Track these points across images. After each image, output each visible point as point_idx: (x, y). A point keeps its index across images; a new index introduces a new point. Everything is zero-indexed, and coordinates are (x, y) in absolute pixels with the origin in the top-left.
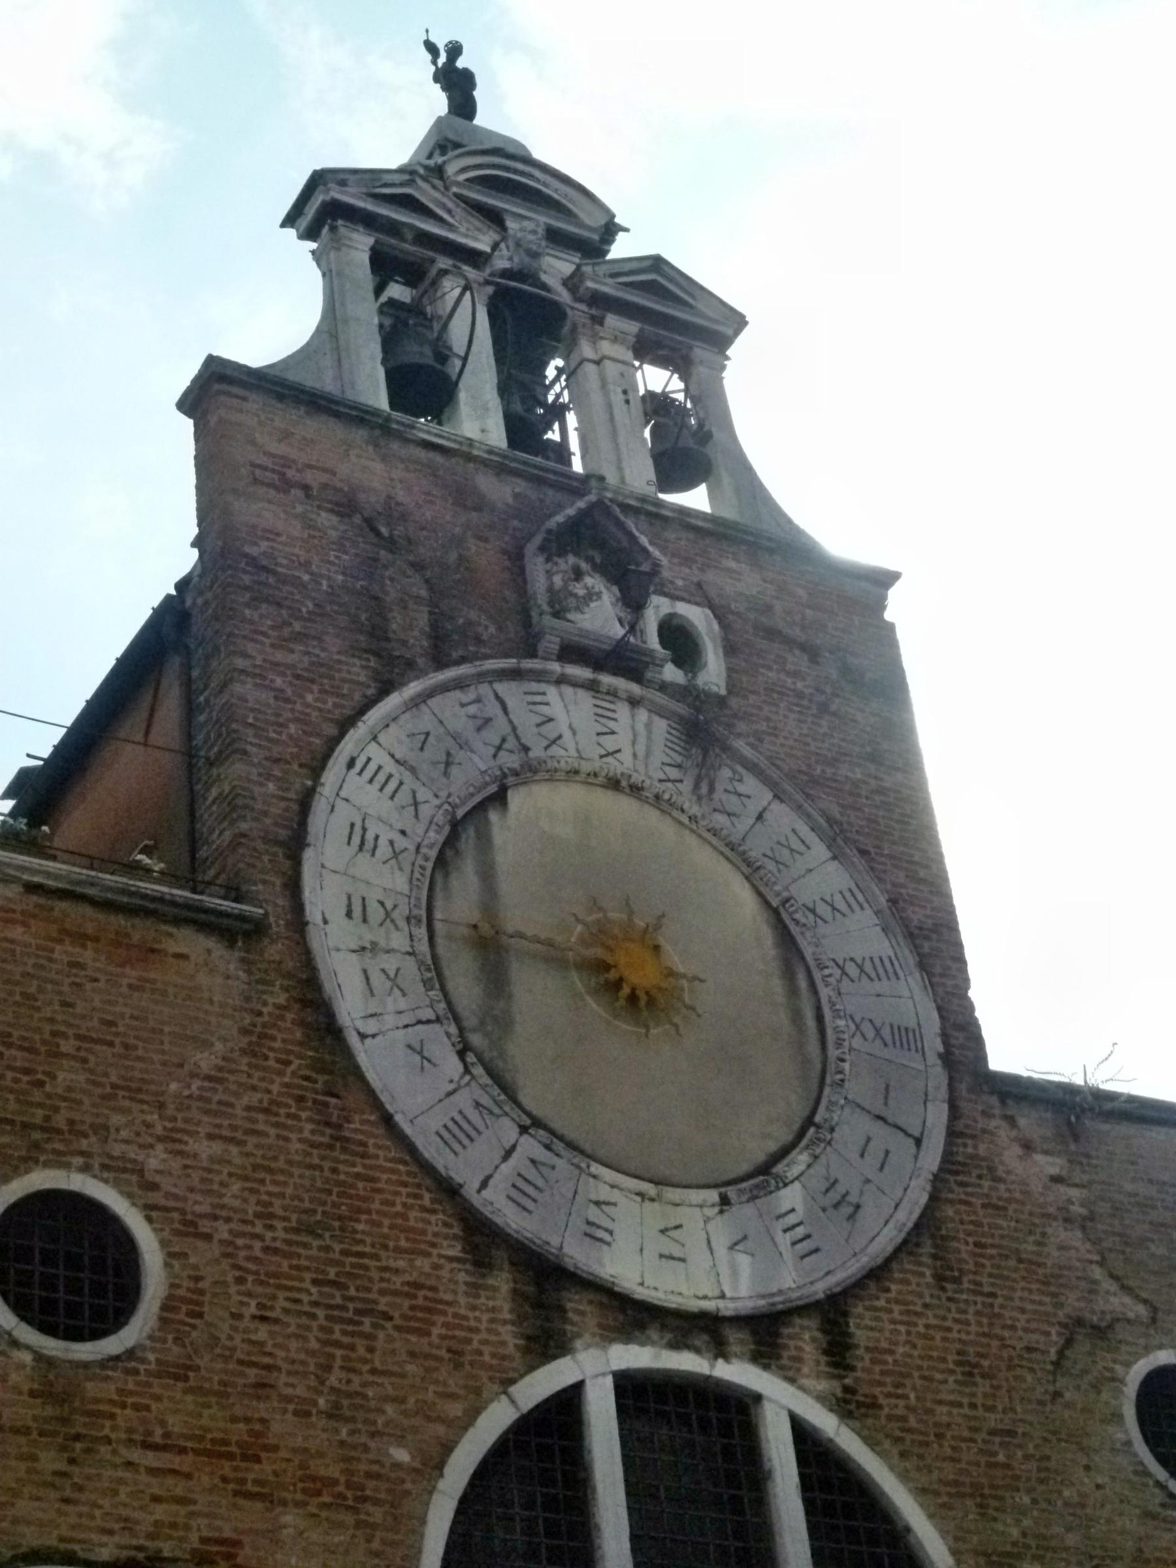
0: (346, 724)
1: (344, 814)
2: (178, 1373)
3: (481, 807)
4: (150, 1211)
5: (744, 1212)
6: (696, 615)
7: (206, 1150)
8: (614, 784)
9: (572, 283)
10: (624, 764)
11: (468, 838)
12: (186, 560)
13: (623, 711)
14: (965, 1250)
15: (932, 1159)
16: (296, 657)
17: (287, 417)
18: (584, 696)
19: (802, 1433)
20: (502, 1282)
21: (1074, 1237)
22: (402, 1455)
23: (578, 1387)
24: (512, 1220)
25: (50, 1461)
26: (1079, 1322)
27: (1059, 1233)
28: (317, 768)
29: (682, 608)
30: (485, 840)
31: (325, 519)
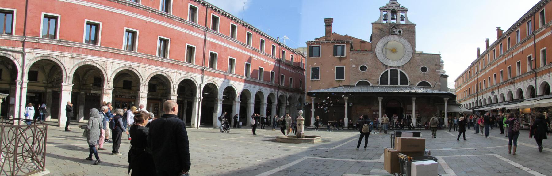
0: (378, 41)
1: (378, 46)
2: (368, 72)
3: (386, 44)
4: (367, 66)
5: (398, 62)
6: (401, 30)
7: (370, 63)
8: (394, 41)
9: (397, 9)
10: (395, 40)
11: (385, 46)
12: (372, 33)
13: (395, 37)
14: (412, 62)
15: (410, 58)
16: (376, 38)
17: (376, 25)
18: (393, 37)
19: (400, 71)
20: (384, 66)
21: (419, 61)
22: (379, 74)
23: (388, 71)
24: (386, 64)
25: (363, 76)
26: (418, 65)
27: (418, 61)
28: (377, 44)
29: (400, 30)
30: (386, 45)
31: (378, 30)
